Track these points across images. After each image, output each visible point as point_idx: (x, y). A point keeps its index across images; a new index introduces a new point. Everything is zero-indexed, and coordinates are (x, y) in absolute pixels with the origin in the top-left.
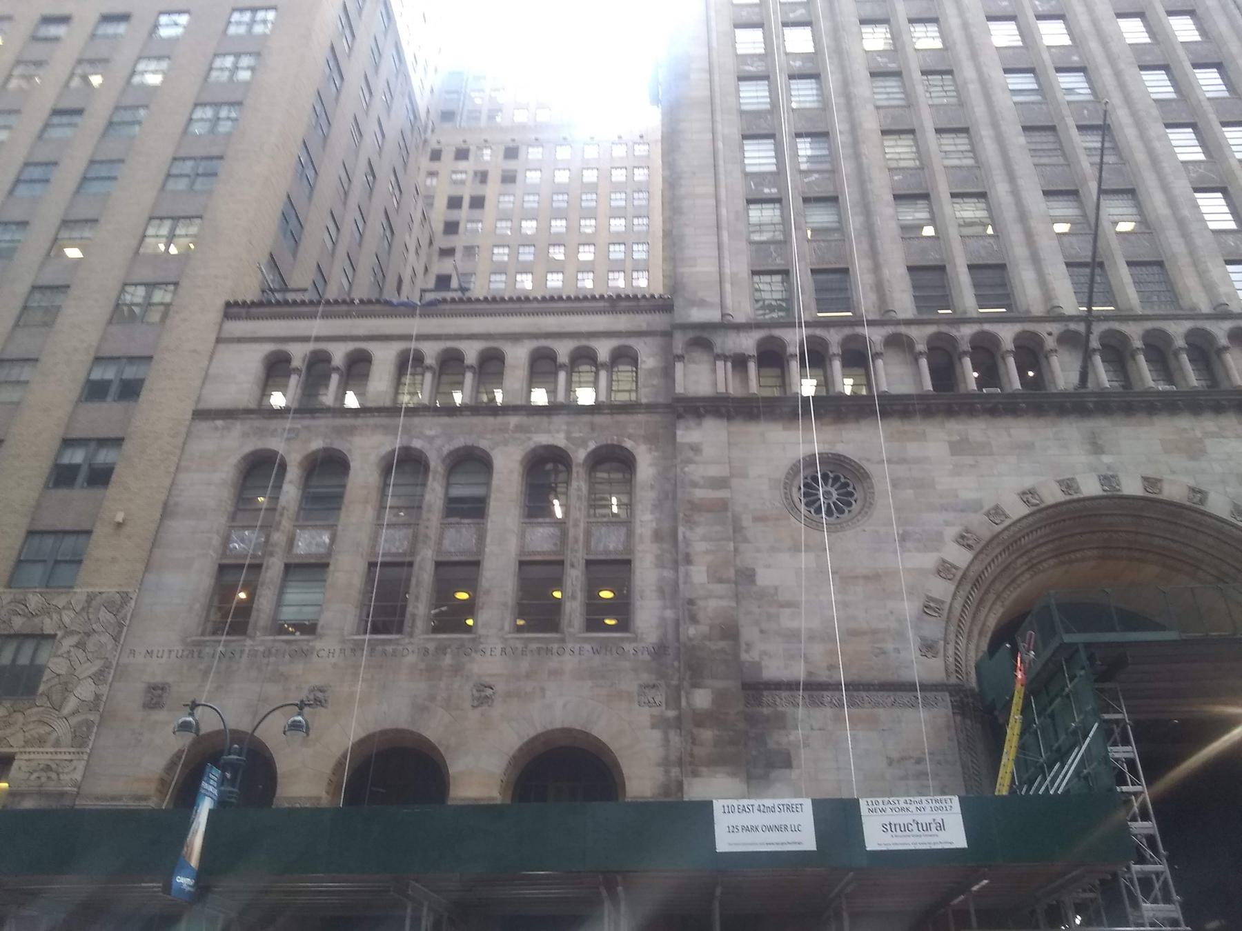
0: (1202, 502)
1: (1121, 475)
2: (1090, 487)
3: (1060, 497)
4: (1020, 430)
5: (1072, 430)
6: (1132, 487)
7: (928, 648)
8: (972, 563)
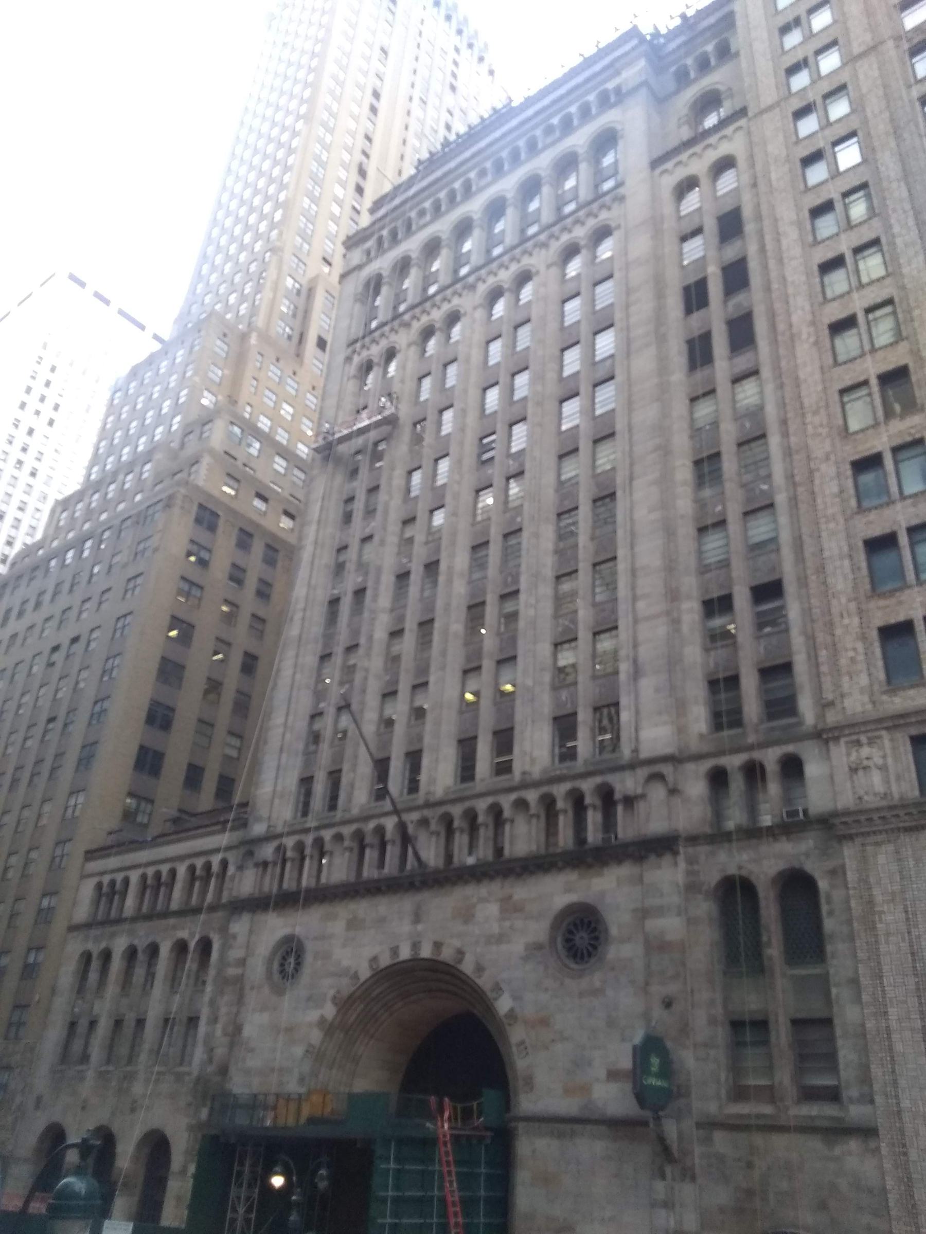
0: (460, 961)
2: (405, 953)
4: (383, 906)
5: (406, 903)
6: (426, 952)
7: (302, 1080)
8: (336, 1016)
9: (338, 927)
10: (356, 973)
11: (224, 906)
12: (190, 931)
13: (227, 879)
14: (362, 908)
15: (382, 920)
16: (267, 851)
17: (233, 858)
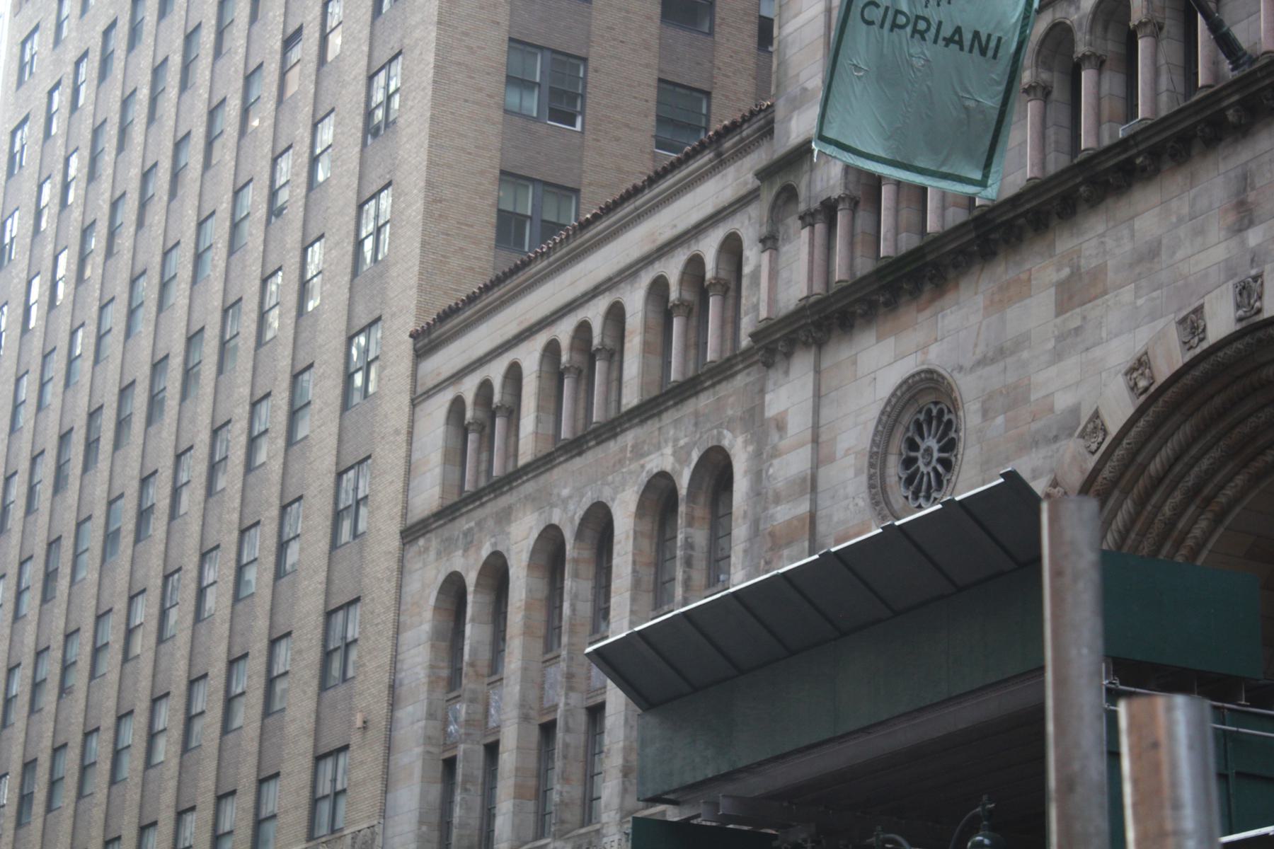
1: (1268, 268)
2: (1221, 321)
3: (1179, 358)
9: (1035, 313)
10: (1096, 415)
11: (747, 353)
12: (669, 451)
13: (745, 282)
14: (1098, 239)
15: (1152, 253)
16: (827, 178)
17: (748, 226)
